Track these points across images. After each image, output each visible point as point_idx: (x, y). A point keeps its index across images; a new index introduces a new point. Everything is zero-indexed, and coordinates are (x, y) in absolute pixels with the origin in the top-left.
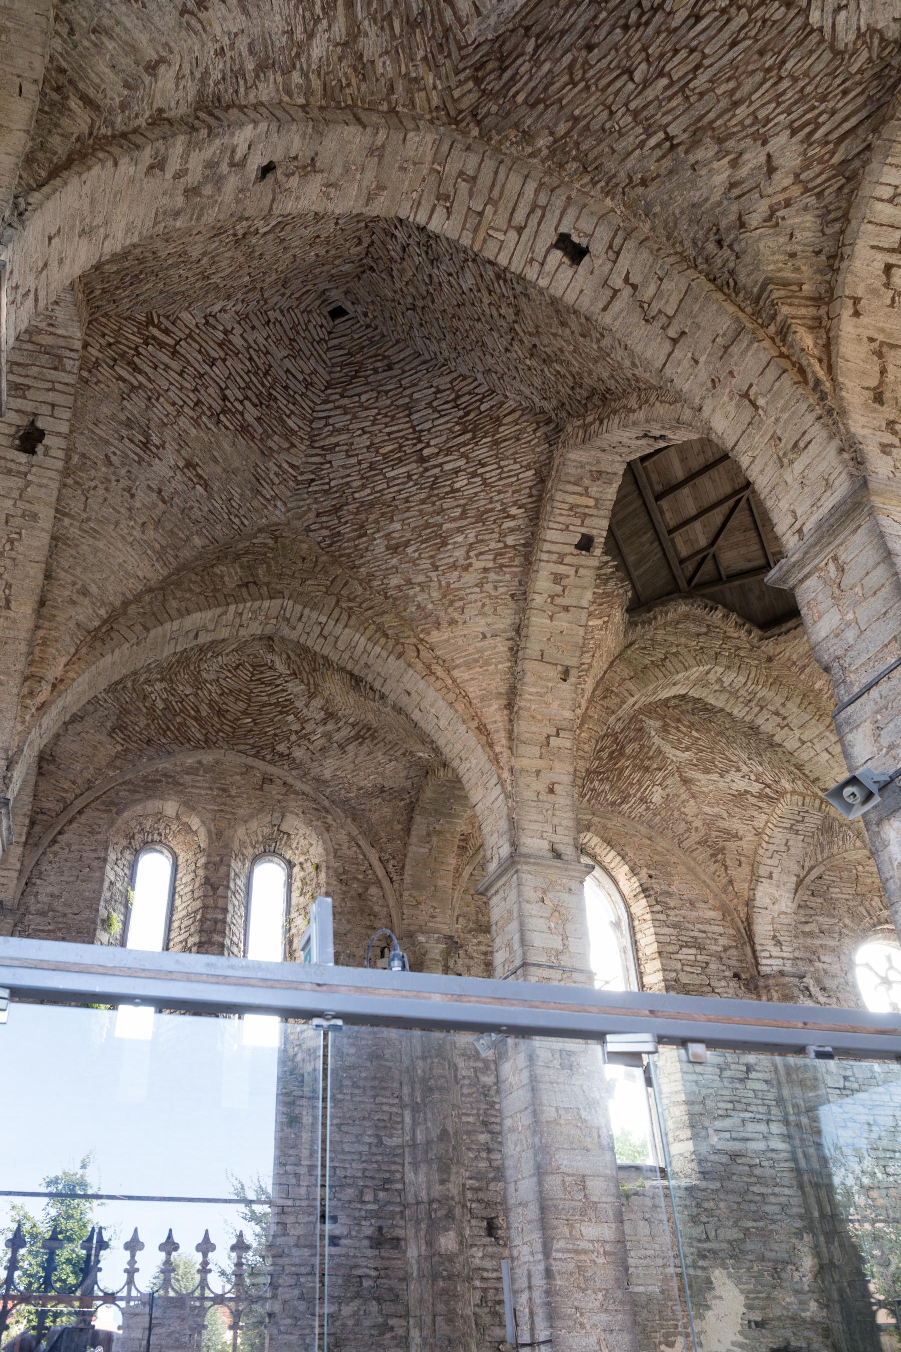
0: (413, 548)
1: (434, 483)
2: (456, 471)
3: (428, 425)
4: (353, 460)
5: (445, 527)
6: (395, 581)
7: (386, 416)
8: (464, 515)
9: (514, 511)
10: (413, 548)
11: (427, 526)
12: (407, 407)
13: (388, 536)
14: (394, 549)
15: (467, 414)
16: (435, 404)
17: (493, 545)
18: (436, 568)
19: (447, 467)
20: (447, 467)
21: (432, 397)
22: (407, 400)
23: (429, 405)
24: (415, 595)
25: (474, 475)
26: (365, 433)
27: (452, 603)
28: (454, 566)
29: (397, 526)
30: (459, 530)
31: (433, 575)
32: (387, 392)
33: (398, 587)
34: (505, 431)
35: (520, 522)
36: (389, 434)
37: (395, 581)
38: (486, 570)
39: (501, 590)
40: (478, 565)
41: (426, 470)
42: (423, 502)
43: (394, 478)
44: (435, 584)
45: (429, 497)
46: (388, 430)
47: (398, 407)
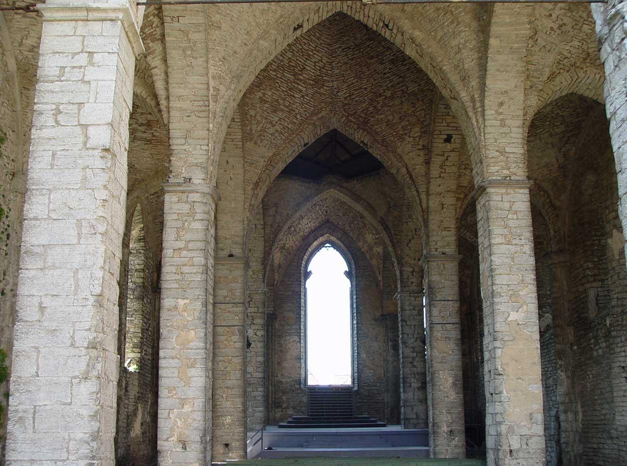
0: (267, 105)
1: (292, 88)
2: (301, 91)
3: (309, 69)
4: (281, 58)
5: (281, 106)
6: (252, 113)
7: (302, 52)
8: (287, 107)
9: (298, 116)
10: (267, 105)
11: (277, 101)
12: (309, 55)
13: (264, 94)
14: (262, 100)
15: (320, 76)
16: (317, 64)
17: (286, 124)
18: (266, 119)
19: (300, 87)
20: (300, 87)
21: (317, 61)
22: (312, 54)
23: (315, 62)
24: (254, 124)
25: (303, 96)
26: (292, 52)
27: (261, 135)
28: (271, 123)
29: (270, 93)
30: (282, 110)
31: (264, 121)
32: (310, 45)
33: (251, 116)
34: (322, 91)
35: (297, 122)
36: (297, 59)
37: (252, 113)
38: (277, 131)
39: (275, 141)
40: (277, 127)
41: (294, 82)
42: (283, 91)
43: (284, 76)
44: (261, 125)
45: (286, 91)
46: (298, 58)
47: (308, 53)
